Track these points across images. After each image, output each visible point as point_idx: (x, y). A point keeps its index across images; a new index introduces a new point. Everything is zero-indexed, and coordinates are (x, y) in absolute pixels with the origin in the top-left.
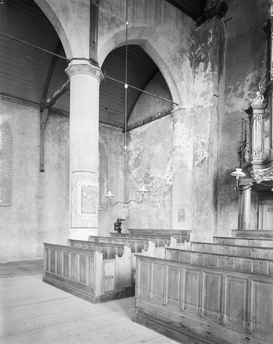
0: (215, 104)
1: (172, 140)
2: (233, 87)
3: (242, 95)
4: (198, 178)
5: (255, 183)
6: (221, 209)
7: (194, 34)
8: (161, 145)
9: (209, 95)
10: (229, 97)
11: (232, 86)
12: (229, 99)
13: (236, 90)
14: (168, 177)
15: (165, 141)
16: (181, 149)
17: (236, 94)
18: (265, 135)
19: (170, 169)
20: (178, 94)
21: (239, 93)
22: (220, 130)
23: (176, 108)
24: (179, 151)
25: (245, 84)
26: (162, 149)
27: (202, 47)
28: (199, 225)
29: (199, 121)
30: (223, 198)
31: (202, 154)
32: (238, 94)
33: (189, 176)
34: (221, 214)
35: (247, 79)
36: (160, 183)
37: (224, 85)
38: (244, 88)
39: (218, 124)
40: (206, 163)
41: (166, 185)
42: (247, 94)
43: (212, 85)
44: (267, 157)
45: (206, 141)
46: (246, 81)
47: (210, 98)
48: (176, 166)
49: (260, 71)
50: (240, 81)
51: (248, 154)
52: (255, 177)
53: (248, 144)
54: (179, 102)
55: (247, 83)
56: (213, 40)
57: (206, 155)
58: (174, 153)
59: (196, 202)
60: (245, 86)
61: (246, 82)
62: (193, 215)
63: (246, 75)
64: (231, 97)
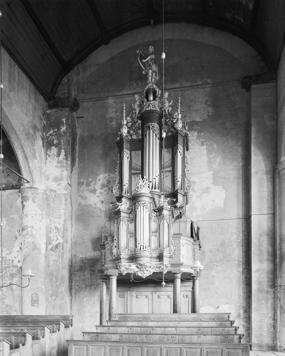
1: (21, 218)
4: (52, 263)
5: (120, 274)
6: (76, 294)
7: (48, 117)
8: (7, 220)
9: (62, 182)
14: (15, 258)
15: (11, 217)
16: (33, 230)
19: (19, 249)
20: (30, 171)
22: (73, 218)
23: (27, 185)
24: (31, 231)
26: (7, 226)
27: (54, 132)
28: (54, 309)
29: (52, 205)
30: (78, 283)
31: (55, 238)
33: (42, 259)
34: (76, 299)
35: (99, 178)
36: (5, 263)
39: (71, 212)
40: (61, 249)
41: (14, 266)
44: (131, 254)
45: (60, 227)
48: (27, 247)
51: (115, 248)
52: (121, 269)
53: (115, 240)
54: (31, 180)
56: (66, 129)
57: (61, 240)
58: (24, 233)
59: (50, 287)
62: (47, 300)
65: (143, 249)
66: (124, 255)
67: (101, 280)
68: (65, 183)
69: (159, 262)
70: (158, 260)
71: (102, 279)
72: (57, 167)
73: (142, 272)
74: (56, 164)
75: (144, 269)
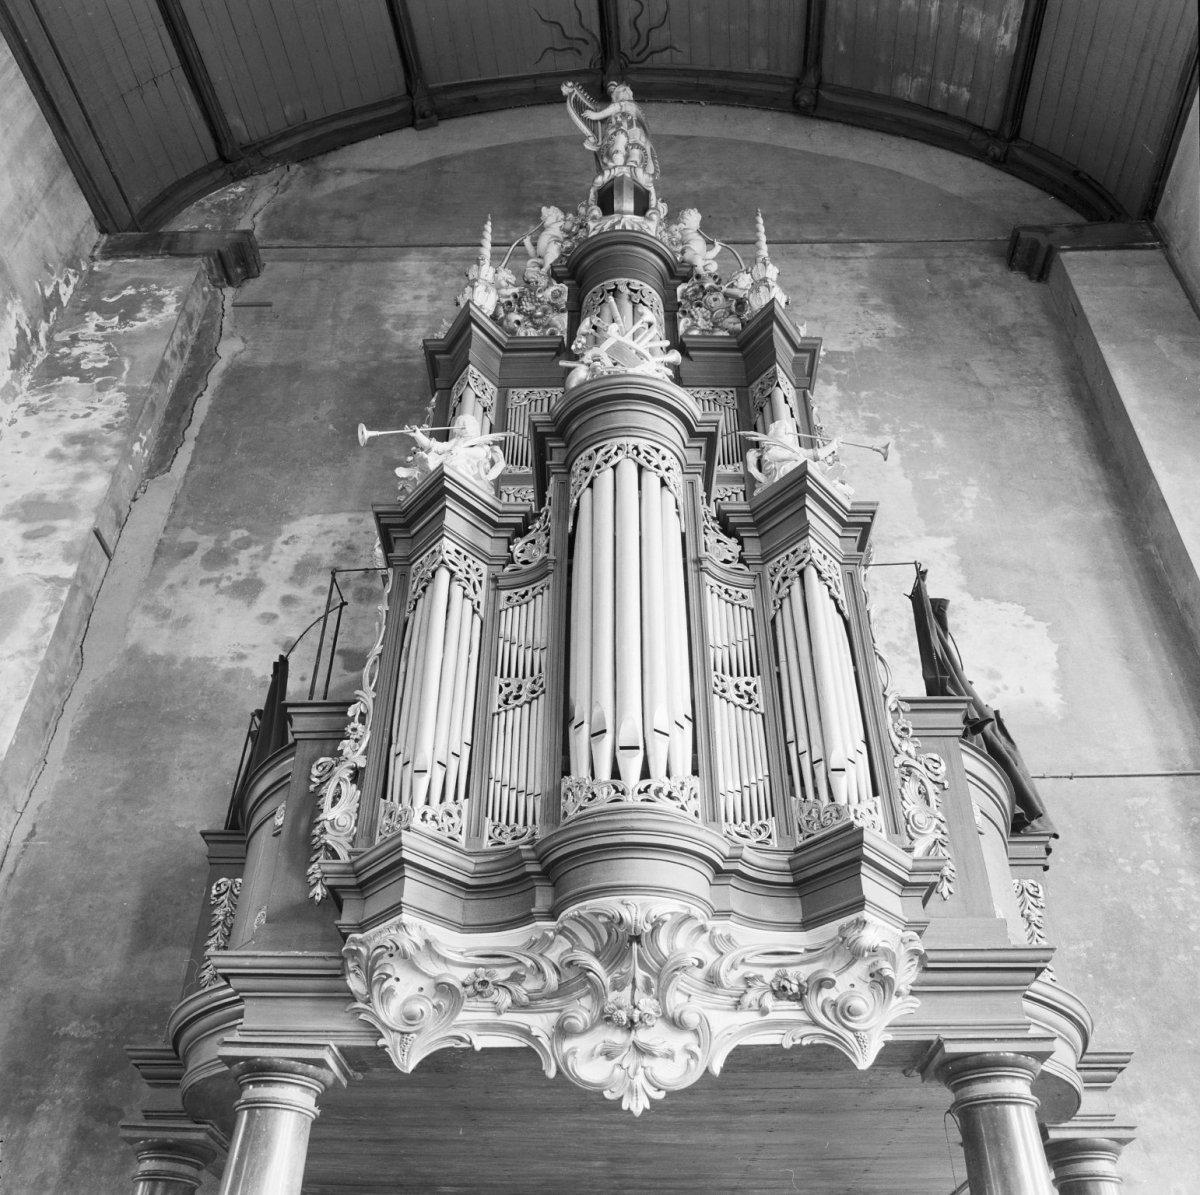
0: (81, 576)
2: (206, 542)
3: (249, 589)
5: (366, 1060)
9: (64, 523)
10: (174, 576)
11: (205, 537)
12: (171, 587)
13: (219, 558)
17: (216, 574)
18: (506, 690)
21: (235, 578)
22: (75, 712)
25: (275, 549)
32: (229, 578)
35: (289, 529)
37: (162, 521)
38: (269, 563)
42: (279, 596)
43: (97, 485)
46: (283, 537)
47: (64, 536)
49: (359, 521)
50: (250, 529)
55: (285, 548)
60: (273, 558)
61: (286, 543)
63: (291, 518)
64: (185, 583)
65: (645, 774)
66: (435, 828)
67: (148, 1165)
68: (75, 529)
69: (806, 925)
70: (793, 911)
71: (162, 1149)
72: (57, 456)
73: (618, 1038)
74: (59, 445)
75: (647, 1004)
